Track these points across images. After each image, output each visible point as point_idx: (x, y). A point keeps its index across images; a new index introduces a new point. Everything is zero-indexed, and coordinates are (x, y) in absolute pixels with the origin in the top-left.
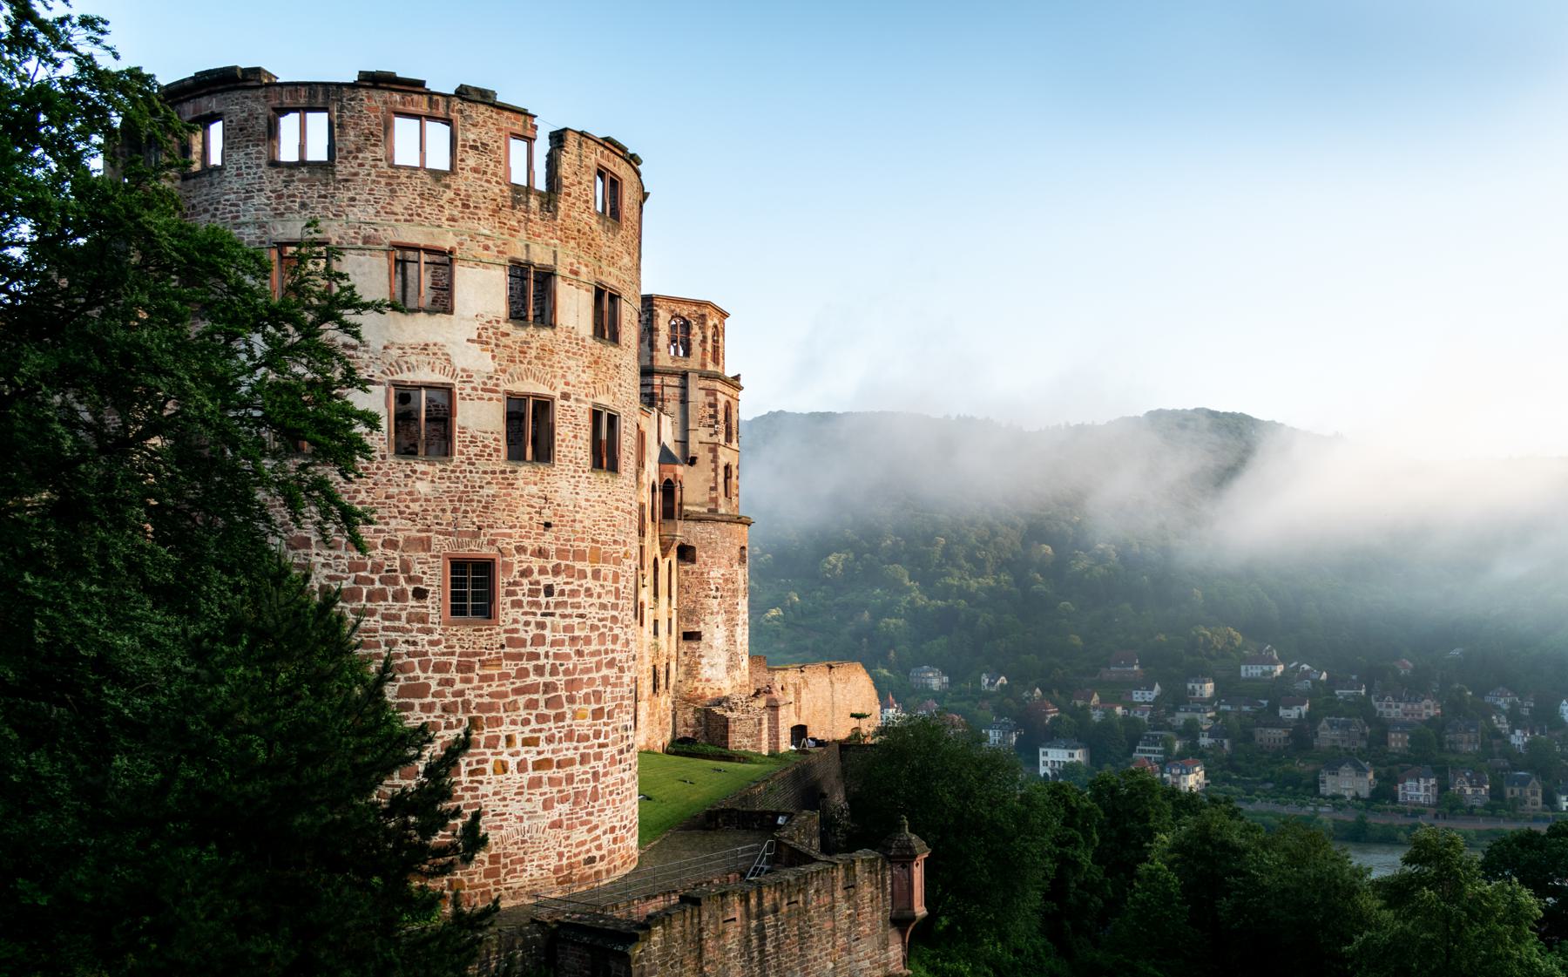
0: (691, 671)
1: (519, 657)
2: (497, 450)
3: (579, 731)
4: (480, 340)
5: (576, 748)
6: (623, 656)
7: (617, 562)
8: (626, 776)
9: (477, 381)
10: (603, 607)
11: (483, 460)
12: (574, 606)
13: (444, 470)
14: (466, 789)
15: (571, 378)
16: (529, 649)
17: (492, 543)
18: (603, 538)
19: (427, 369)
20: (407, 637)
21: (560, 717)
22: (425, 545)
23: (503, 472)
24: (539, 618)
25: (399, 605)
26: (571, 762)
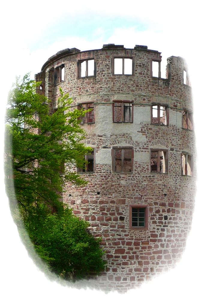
4: (142, 131)
9: (141, 145)
12: (175, 223)
15: (174, 143)
17: (146, 201)
19: (124, 142)
20: (118, 233)
23: (149, 177)
24: (162, 227)
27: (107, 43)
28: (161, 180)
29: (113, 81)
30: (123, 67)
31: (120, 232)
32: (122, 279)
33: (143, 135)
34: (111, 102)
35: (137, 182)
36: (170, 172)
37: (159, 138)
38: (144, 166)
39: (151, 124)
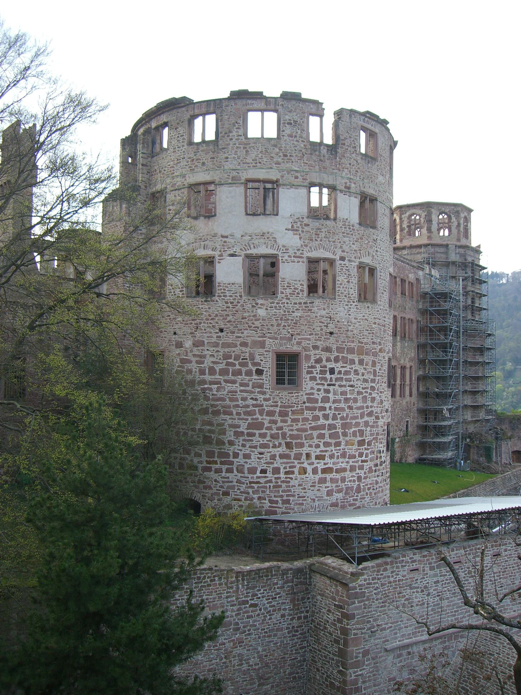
1: (314, 409)
2: (302, 291)
3: (349, 452)
4: (293, 229)
5: (348, 462)
7: (375, 355)
8: (379, 479)
9: (291, 252)
10: (365, 381)
12: (347, 380)
13: (273, 303)
14: (283, 482)
16: (320, 404)
17: (299, 343)
19: (264, 246)
20: (252, 396)
21: (338, 444)
22: (262, 345)
23: (305, 303)
24: (326, 387)
25: (248, 378)
26: (344, 470)
27: (236, 89)
28: (324, 309)
29: (246, 148)
30: (262, 125)
31: (256, 394)
32: (258, 472)
33: (294, 234)
34: (242, 181)
35: (285, 311)
36: (339, 295)
37: (321, 241)
38: (296, 286)
39: (308, 217)
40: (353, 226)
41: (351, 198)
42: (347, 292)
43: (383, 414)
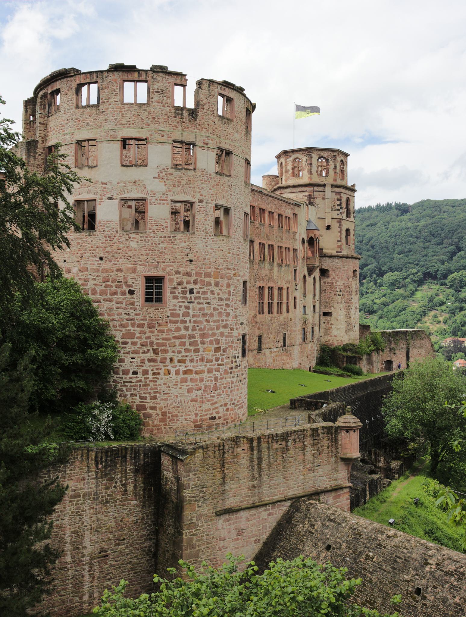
0: (327, 331)
1: (176, 322)
2: (167, 227)
4: (159, 178)
5: (205, 366)
6: (233, 323)
7: (230, 278)
8: (235, 380)
9: (158, 196)
10: (221, 299)
11: (160, 232)
12: (204, 299)
13: (143, 237)
14: (151, 381)
15: (203, 192)
17: (164, 270)
18: (221, 267)
20: (126, 311)
21: (197, 351)
24: (186, 304)
26: (202, 372)
29: (121, 112)
31: (129, 310)
35: (152, 244)
36: (197, 231)
37: (183, 187)
38: (162, 223)
39: (172, 168)
40: (210, 175)
41: (209, 152)
42: (204, 228)
43: (238, 327)
